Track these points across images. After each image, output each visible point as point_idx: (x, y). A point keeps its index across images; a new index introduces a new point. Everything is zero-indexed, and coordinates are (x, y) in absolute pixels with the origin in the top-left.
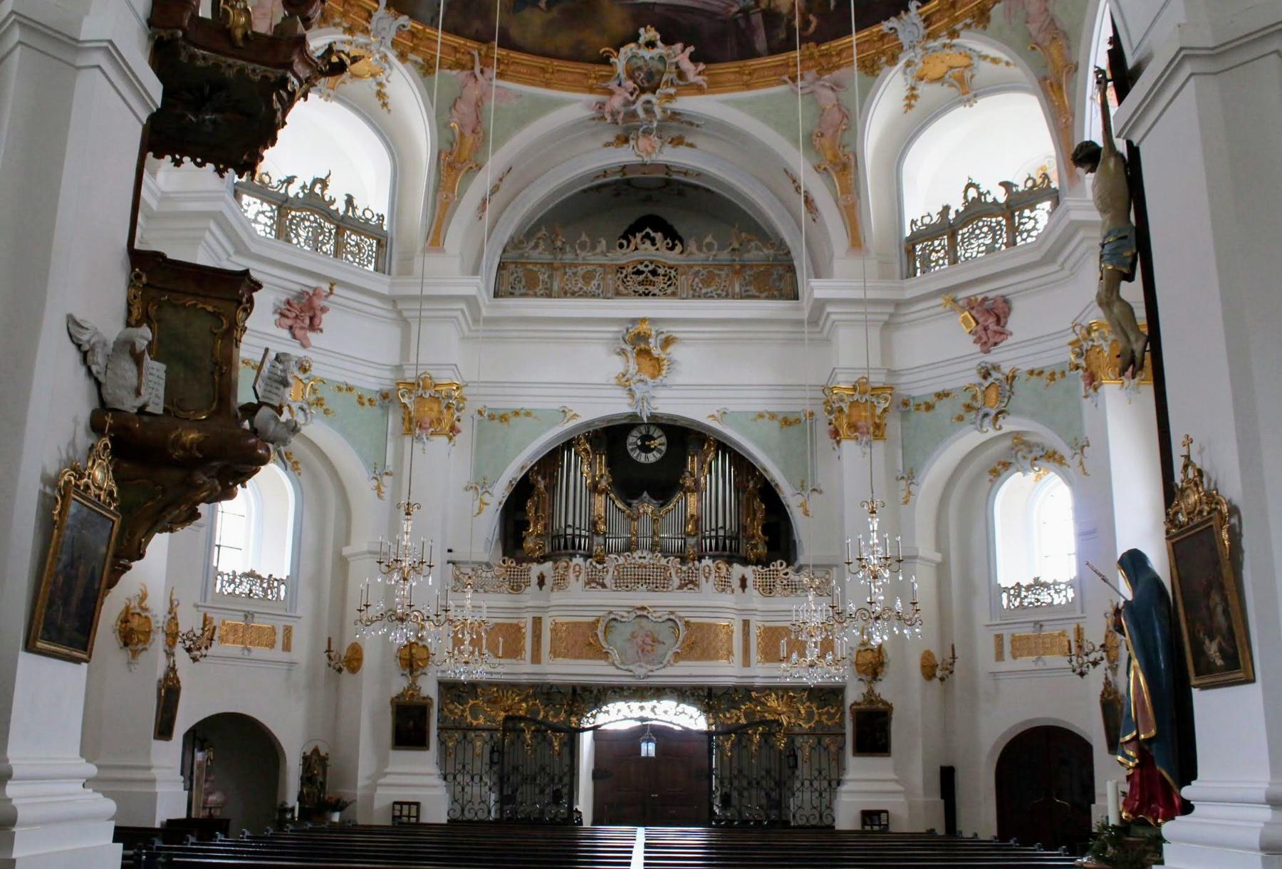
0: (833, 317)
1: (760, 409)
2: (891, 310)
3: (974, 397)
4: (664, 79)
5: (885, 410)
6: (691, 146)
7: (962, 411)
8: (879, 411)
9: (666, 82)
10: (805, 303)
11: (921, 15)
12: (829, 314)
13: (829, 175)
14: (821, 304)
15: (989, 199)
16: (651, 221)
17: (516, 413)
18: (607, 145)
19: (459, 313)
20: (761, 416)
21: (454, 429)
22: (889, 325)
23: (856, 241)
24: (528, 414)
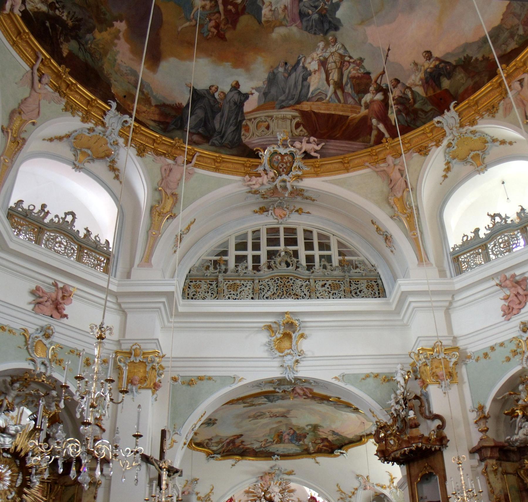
0: (413, 305)
1: (368, 371)
2: (449, 298)
3: (518, 346)
4: (294, 166)
5: (456, 363)
6: (308, 213)
7: (511, 355)
8: (451, 364)
9: (296, 167)
10: (393, 297)
11: (456, 111)
12: (410, 302)
13: (401, 221)
14: (405, 295)
15: (509, 221)
16: (282, 263)
17: (201, 379)
18: (255, 212)
19: (161, 305)
20: (368, 376)
21: (156, 387)
22: (448, 311)
23: (422, 258)
24: (210, 378)
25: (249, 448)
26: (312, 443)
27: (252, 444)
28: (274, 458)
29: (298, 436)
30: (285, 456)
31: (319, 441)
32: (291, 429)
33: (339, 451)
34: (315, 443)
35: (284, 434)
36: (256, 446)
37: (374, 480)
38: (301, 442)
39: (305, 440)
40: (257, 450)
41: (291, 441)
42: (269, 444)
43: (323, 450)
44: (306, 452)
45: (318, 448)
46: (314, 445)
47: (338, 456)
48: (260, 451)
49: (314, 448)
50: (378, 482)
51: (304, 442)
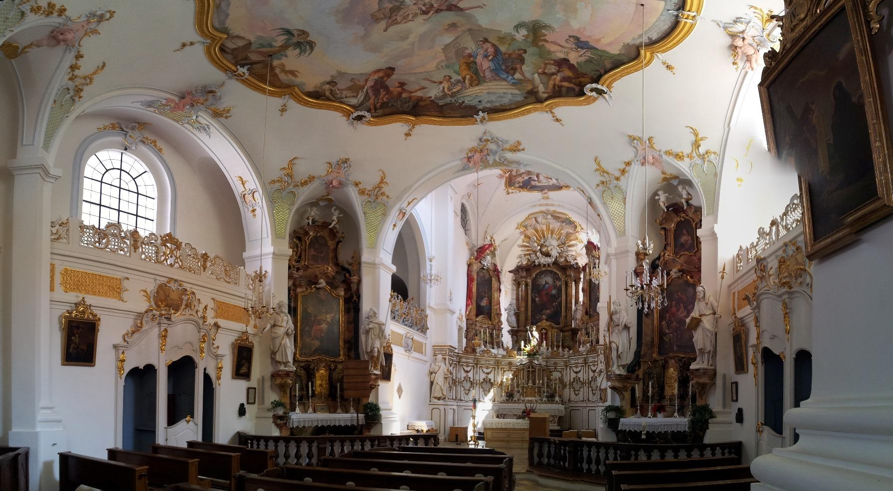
25: (421, 99)
26: (539, 74)
27: (424, 88)
28: (478, 118)
29: (507, 63)
30: (497, 111)
31: (553, 69)
32: (486, 40)
33: (594, 85)
34: (544, 73)
35: (479, 59)
36: (433, 92)
37: (662, 145)
38: (517, 76)
39: (524, 68)
40: (441, 103)
41: (496, 73)
42: (459, 88)
43: (564, 90)
44: (533, 98)
45: (554, 85)
46: (544, 78)
47: (595, 99)
48: (446, 105)
49: (546, 85)
50: (669, 149)
51: (522, 74)
